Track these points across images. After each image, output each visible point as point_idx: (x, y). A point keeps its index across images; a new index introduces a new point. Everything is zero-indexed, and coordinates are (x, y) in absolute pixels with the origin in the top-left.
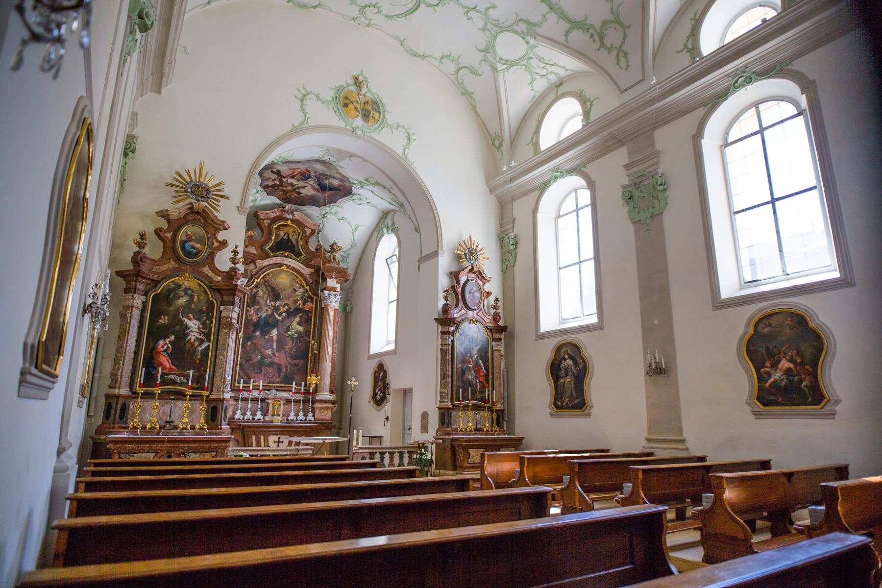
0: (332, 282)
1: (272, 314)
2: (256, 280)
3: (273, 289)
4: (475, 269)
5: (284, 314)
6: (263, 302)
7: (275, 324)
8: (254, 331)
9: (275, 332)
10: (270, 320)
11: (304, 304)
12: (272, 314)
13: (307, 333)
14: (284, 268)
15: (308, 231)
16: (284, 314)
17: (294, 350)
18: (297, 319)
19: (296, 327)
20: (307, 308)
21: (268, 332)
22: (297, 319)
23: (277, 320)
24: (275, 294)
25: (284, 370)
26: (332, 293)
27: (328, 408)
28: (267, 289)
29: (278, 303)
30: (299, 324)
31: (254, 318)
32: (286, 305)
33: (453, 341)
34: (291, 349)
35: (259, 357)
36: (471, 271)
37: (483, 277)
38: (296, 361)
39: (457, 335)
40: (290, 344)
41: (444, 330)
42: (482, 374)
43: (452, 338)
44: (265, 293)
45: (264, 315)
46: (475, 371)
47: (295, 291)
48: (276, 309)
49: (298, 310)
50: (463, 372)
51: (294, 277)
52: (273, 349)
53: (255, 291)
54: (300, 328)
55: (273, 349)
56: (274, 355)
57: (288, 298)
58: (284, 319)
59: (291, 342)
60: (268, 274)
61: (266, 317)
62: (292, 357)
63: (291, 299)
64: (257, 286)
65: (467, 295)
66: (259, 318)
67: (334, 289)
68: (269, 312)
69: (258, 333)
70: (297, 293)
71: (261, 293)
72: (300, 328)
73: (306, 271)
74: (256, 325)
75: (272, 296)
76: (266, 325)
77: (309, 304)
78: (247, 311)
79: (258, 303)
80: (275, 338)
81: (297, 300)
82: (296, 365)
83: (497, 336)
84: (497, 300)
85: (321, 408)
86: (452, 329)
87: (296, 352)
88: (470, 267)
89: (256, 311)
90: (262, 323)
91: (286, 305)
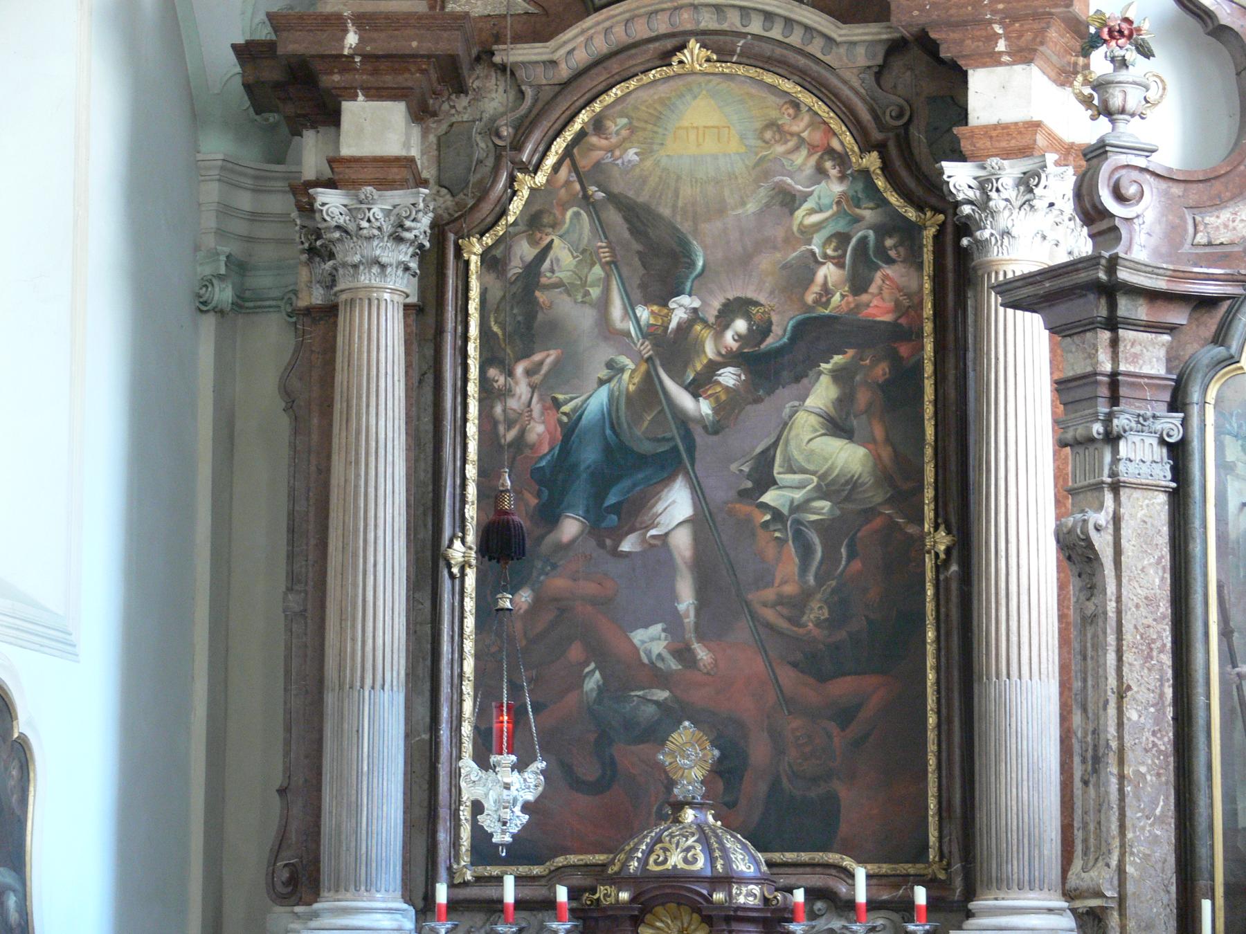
0: (999, 94)
1: (650, 391)
2: (526, 184)
3: (638, 217)
5: (729, 377)
6: (582, 319)
7: (670, 461)
8: (550, 516)
9: (676, 505)
10: (640, 435)
11: (858, 285)
12: (650, 391)
13: (899, 478)
14: (694, 54)
16: (729, 377)
17: (817, 611)
18: (822, 393)
19: (818, 447)
20: (878, 305)
21: (634, 512)
22: (822, 393)
23: (683, 421)
24: (658, 255)
25: (759, 751)
26: (1009, 172)
28: (601, 227)
29: (681, 307)
30: (837, 426)
31: (537, 430)
32: (730, 311)
34: (797, 605)
35: (593, 682)
38: (842, 688)
39: (1209, 398)
40: (787, 575)
41: (1081, 368)
43: (1171, 425)
44: (587, 257)
45: (598, 400)
47: (789, 201)
48: (673, 348)
49: (818, 334)
51: (773, 109)
52: (674, 624)
53: (525, 250)
54: (848, 457)
55: (674, 624)
56: (683, 653)
57: (744, 262)
58: (729, 407)
59: (789, 564)
60: (598, 124)
61: (611, 418)
62: (817, 664)
63: (766, 262)
64: (534, 221)
66: (570, 430)
67: (1020, 140)
68: (629, 381)
69: (570, 527)
70: (804, 216)
71: (563, 257)
72: (848, 457)
74: (554, 482)
75: (635, 271)
76: (620, 465)
78: (488, 393)
79: (554, 331)
80: (682, 542)
81: (814, 261)
82: (845, 715)
86: (1146, 356)
87: (833, 623)
89: (548, 386)
90: (589, 455)
91: (730, 311)
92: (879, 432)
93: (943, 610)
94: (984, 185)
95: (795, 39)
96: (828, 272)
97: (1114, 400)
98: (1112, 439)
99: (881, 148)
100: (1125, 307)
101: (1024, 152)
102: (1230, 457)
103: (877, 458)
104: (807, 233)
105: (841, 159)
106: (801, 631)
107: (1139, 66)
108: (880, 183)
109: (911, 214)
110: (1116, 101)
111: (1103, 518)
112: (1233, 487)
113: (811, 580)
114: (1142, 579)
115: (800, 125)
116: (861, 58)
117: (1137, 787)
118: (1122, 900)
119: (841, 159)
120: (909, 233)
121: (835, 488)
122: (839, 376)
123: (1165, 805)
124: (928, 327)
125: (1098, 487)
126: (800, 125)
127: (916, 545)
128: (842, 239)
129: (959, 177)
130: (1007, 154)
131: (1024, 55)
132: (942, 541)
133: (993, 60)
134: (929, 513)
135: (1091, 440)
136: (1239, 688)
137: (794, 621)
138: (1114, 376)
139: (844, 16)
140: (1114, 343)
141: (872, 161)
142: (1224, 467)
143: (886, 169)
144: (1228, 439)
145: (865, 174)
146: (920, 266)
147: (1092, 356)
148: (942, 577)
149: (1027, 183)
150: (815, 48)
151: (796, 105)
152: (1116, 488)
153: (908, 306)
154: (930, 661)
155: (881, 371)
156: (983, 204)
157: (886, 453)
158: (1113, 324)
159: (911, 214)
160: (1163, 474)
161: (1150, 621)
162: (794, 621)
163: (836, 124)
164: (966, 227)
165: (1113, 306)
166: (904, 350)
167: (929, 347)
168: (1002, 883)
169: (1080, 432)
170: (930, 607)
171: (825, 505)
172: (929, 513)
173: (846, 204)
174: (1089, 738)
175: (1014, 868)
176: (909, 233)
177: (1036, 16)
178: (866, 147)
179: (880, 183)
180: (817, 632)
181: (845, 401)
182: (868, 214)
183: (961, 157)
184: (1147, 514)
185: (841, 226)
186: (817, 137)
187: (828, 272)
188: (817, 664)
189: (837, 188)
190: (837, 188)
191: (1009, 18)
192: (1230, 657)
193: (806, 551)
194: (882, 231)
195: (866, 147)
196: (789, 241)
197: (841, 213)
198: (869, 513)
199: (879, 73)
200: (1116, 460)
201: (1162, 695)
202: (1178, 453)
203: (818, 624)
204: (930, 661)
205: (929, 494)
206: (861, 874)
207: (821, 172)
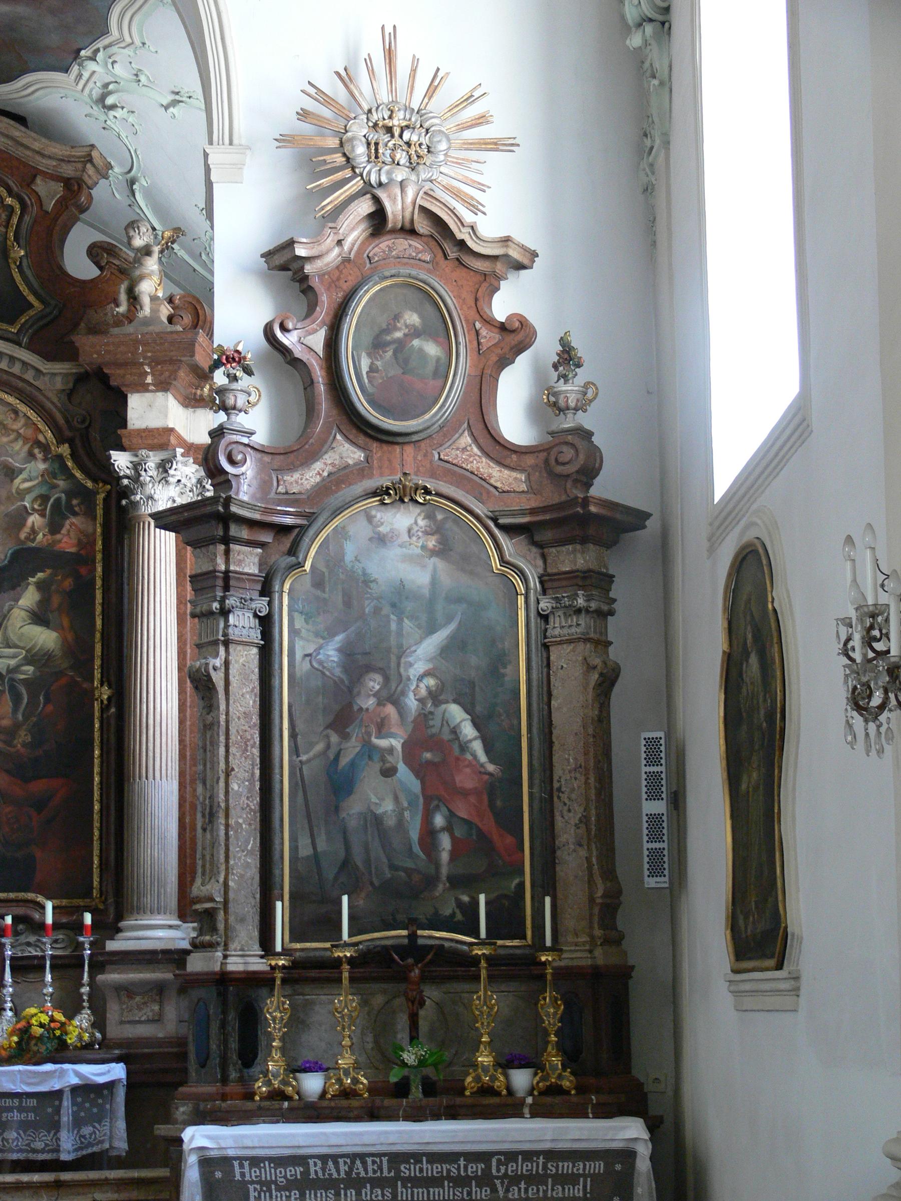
0: (146, 410)
4: (396, 208)
11: (54, 527)
13: (77, 651)
15: (49, 192)
17: (23, 737)
18: (29, 597)
20: (67, 542)
22: (29, 597)
27: (159, 990)
30: (39, 617)
33: (266, 623)
36: (378, 220)
37: (462, 244)
38: (39, 786)
41: (206, 567)
42: (465, 780)
43: (261, 605)
46: (419, 770)
50: (340, 784)
54: (46, 638)
62: (23, 771)
65: (356, 366)
67: (161, 439)
70: (20, 483)
72: (46, 638)
73: (53, 375)
77: (74, 525)
81: (24, 513)
82: (40, 804)
83: (572, 559)
84: (567, 358)
85: (126, 991)
86: (247, 562)
88: (365, 207)
92: (66, 622)
93: (105, 736)
94: (137, 467)
95: (16, 369)
96: (34, 519)
97: (226, 588)
98: (225, 612)
99: (71, 442)
100: (234, 530)
101: (162, 446)
102: (297, 626)
103: (64, 640)
104: (22, 494)
105: (45, 448)
106: (12, 750)
107: (245, 381)
108: (70, 464)
109: (89, 484)
110: (230, 401)
111: (218, 662)
112: (299, 644)
113: (20, 717)
114: (243, 701)
115: (18, 425)
116: (59, 383)
117: (236, 832)
118: (226, 903)
119: (45, 448)
120: (88, 497)
121: (34, 657)
122: (40, 586)
123: (254, 844)
124: (99, 556)
125: (215, 643)
126: (18, 425)
127: (90, 695)
128: (44, 498)
129: (121, 460)
130: (152, 448)
131: (163, 386)
132: (105, 693)
133: (143, 388)
134: (97, 675)
135: (211, 613)
136: (301, 769)
137: (9, 743)
138: (227, 572)
139: (48, 357)
140: (227, 552)
141: (64, 450)
142: (293, 632)
143: (74, 455)
144: (296, 615)
145: (60, 458)
146: (94, 518)
147: (213, 561)
148: (105, 716)
149: (164, 467)
150: (29, 376)
151: (16, 412)
152: (227, 643)
153: (86, 543)
154: (96, 769)
155: (68, 583)
156: (136, 478)
157: (70, 637)
158: (227, 540)
159: (89, 484)
160: (256, 635)
161: (246, 728)
162: (9, 743)
163: (41, 425)
164: (125, 493)
165: (226, 529)
166: (83, 571)
167: (99, 569)
168: (140, 910)
169: (205, 608)
170: (97, 735)
171: (30, 669)
172: (97, 675)
173: (48, 477)
174: (207, 802)
175: (148, 900)
176: (88, 497)
177: (172, 361)
178: (60, 441)
179: (70, 464)
180: (22, 750)
181: (44, 603)
182: (61, 483)
183: (122, 448)
184: (245, 660)
185: (43, 490)
186: (29, 433)
187: (34, 519)
188: (23, 771)
189: (42, 466)
190: (42, 466)
191: (155, 362)
192: (295, 750)
193: (16, 698)
194: (70, 494)
195: (60, 441)
196: (10, 498)
197: (44, 482)
198: (61, 674)
199: (70, 394)
200: (227, 626)
201: (253, 774)
202: (266, 623)
203: (24, 745)
204: (96, 769)
205: (98, 662)
206: (49, 906)
207: (31, 455)
